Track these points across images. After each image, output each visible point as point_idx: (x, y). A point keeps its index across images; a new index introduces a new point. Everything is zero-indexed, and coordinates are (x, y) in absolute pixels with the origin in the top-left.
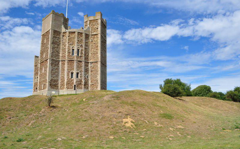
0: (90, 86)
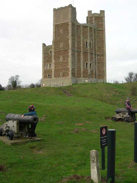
0: (97, 75)
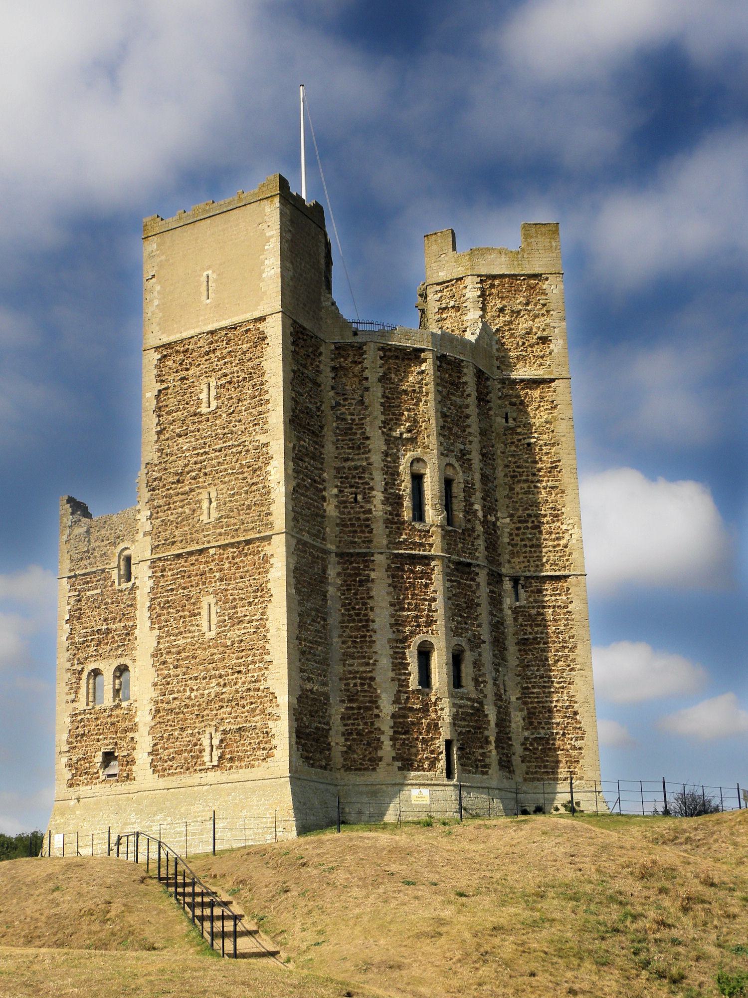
0: (518, 749)
